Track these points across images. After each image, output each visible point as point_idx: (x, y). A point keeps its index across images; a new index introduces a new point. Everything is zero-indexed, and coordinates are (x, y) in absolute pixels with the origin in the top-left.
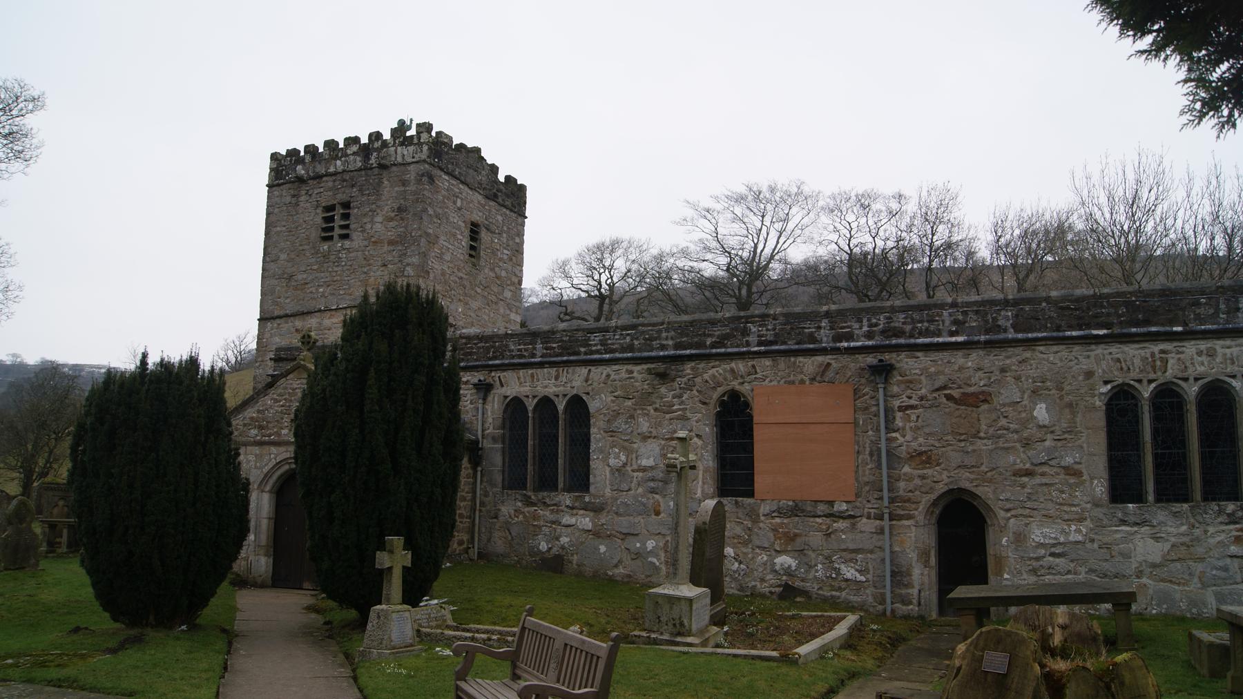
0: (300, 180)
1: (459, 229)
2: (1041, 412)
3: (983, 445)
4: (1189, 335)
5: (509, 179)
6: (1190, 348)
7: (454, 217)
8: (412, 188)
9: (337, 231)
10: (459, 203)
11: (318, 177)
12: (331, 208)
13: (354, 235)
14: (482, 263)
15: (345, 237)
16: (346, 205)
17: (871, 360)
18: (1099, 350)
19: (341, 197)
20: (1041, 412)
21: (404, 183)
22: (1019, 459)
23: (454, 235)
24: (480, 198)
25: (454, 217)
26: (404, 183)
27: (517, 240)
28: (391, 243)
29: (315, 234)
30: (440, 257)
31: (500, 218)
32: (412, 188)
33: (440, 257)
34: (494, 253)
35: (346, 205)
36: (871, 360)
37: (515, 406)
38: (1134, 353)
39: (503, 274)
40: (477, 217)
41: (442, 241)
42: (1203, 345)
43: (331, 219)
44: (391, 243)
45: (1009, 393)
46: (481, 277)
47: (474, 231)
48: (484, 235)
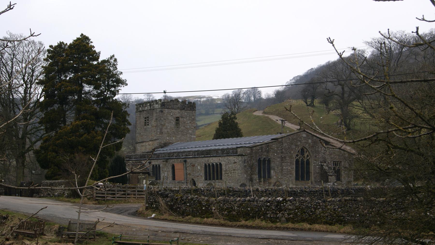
0: (140, 111)
1: (172, 120)
2: (199, 168)
3: (194, 172)
4: (210, 157)
5: (189, 102)
6: (211, 158)
7: (170, 118)
8: (158, 114)
9: (147, 124)
10: (171, 114)
11: (143, 111)
12: (146, 118)
13: (150, 125)
14: (180, 126)
15: (148, 125)
16: (148, 117)
17: (184, 160)
18: (204, 159)
19: (147, 116)
20: (199, 168)
21: (157, 113)
22: (197, 174)
23: (171, 122)
24: (178, 111)
25: (170, 118)
26: (157, 113)
27: (193, 117)
28: (155, 127)
29: (143, 124)
30: (166, 128)
31: (186, 114)
32: (158, 114)
33: (166, 128)
34: (184, 123)
35: (148, 117)
36: (184, 160)
37: (153, 166)
38: (206, 159)
39: (188, 127)
40: (178, 115)
41: (167, 124)
42: (212, 158)
43: (146, 121)
44: (155, 127)
45: (196, 165)
46: (180, 129)
47: (177, 119)
48: (181, 119)
